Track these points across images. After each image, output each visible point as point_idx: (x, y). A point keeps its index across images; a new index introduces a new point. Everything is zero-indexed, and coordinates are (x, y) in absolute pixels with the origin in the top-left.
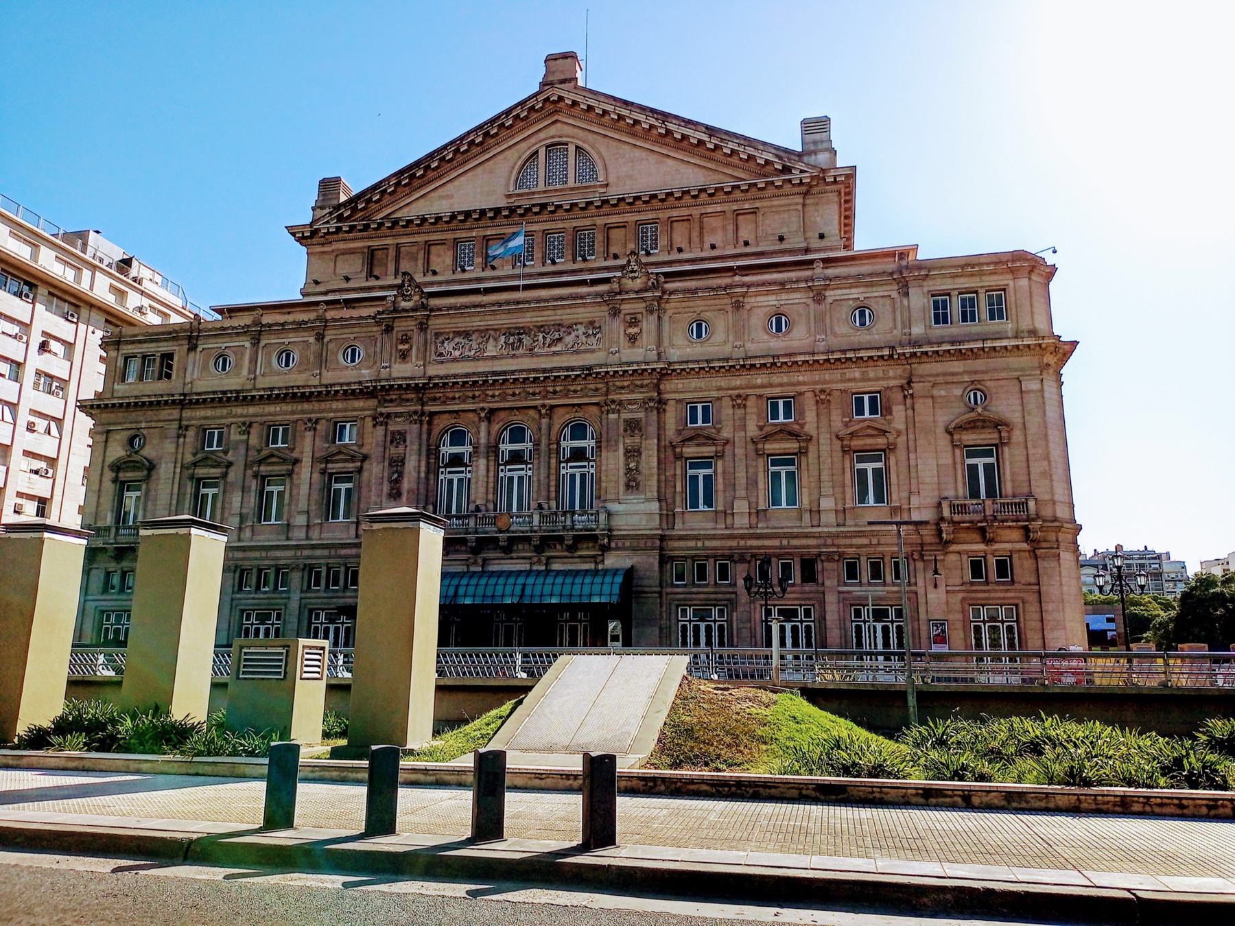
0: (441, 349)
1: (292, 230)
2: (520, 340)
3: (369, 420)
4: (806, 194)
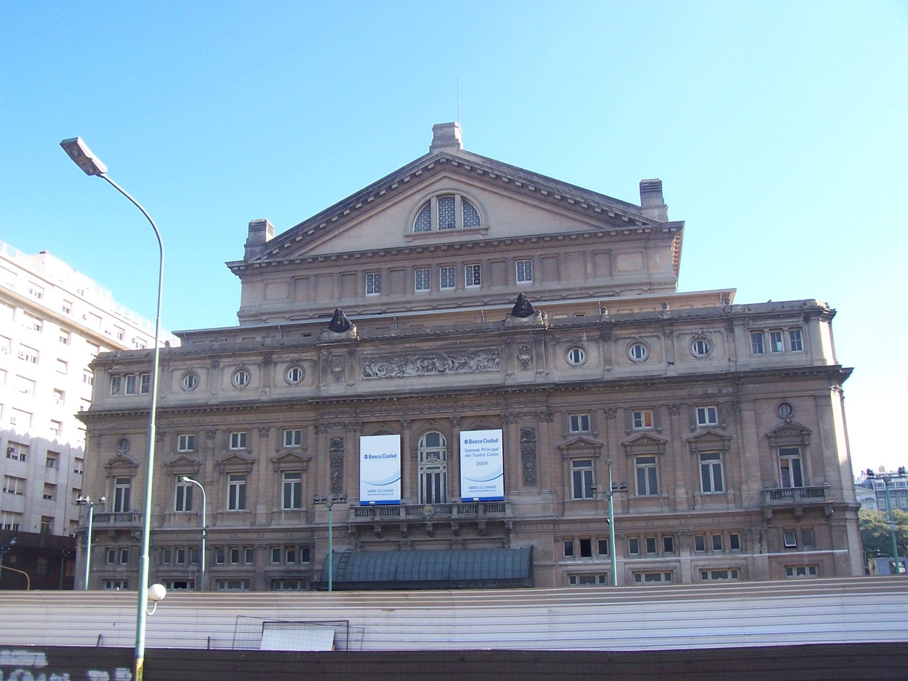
0: (368, 371)
1: (232, 266)
2: (434, 364)
3: (311, 428)
4: (648, 239)
